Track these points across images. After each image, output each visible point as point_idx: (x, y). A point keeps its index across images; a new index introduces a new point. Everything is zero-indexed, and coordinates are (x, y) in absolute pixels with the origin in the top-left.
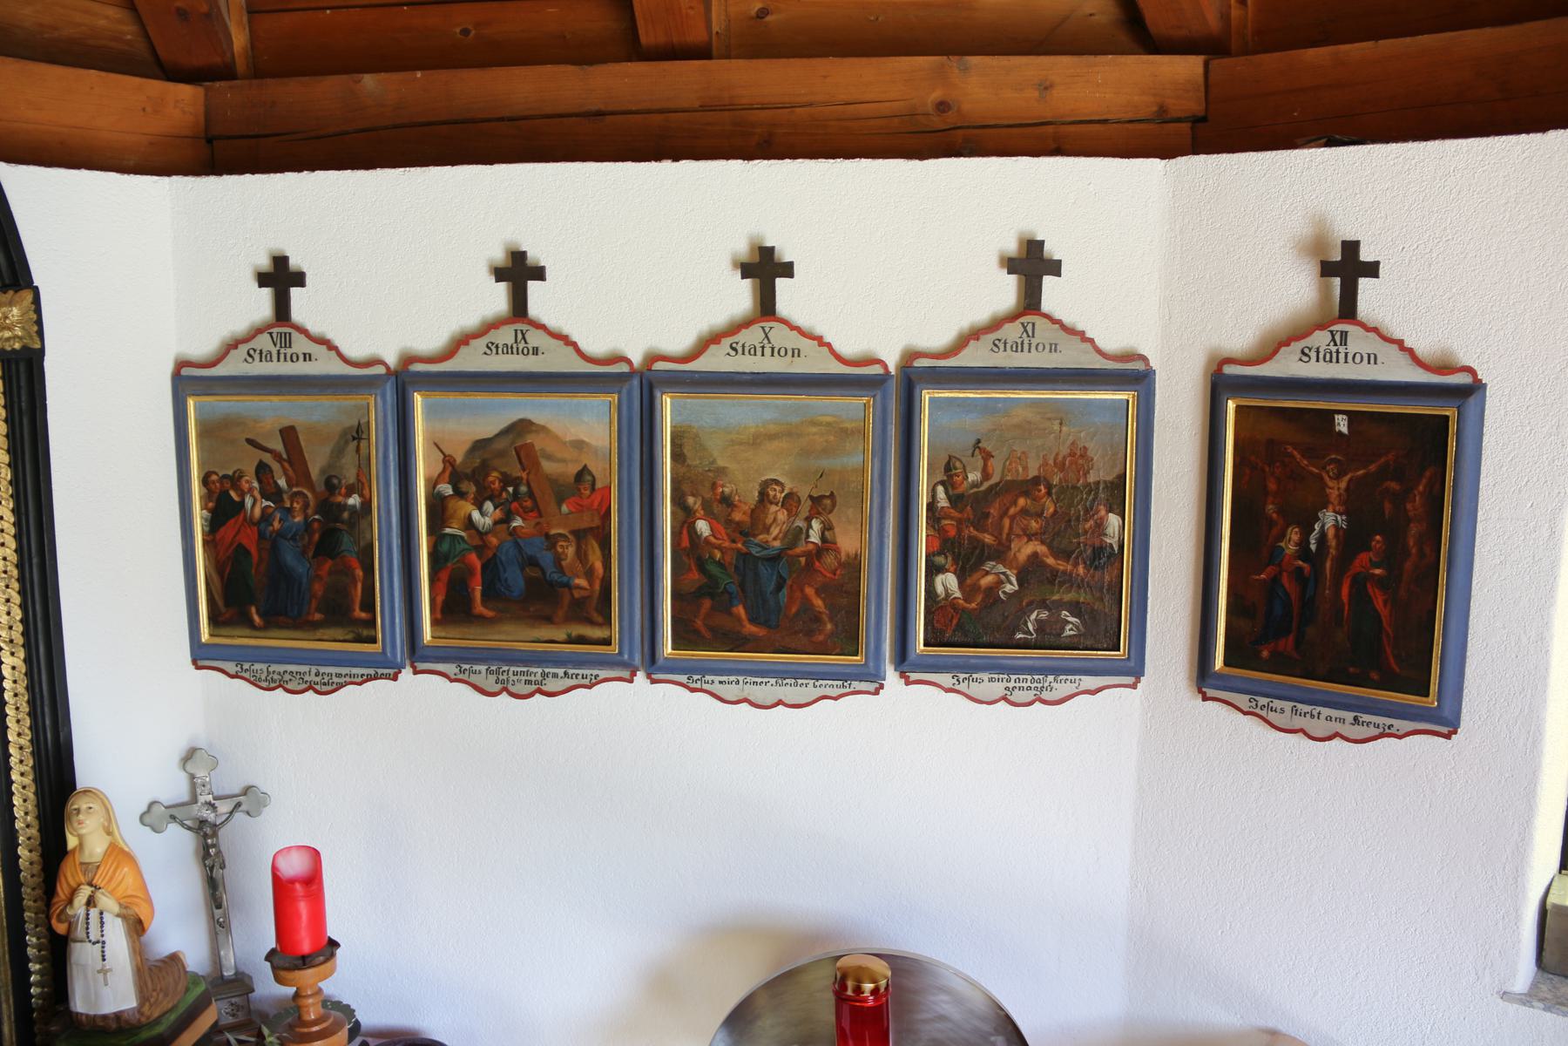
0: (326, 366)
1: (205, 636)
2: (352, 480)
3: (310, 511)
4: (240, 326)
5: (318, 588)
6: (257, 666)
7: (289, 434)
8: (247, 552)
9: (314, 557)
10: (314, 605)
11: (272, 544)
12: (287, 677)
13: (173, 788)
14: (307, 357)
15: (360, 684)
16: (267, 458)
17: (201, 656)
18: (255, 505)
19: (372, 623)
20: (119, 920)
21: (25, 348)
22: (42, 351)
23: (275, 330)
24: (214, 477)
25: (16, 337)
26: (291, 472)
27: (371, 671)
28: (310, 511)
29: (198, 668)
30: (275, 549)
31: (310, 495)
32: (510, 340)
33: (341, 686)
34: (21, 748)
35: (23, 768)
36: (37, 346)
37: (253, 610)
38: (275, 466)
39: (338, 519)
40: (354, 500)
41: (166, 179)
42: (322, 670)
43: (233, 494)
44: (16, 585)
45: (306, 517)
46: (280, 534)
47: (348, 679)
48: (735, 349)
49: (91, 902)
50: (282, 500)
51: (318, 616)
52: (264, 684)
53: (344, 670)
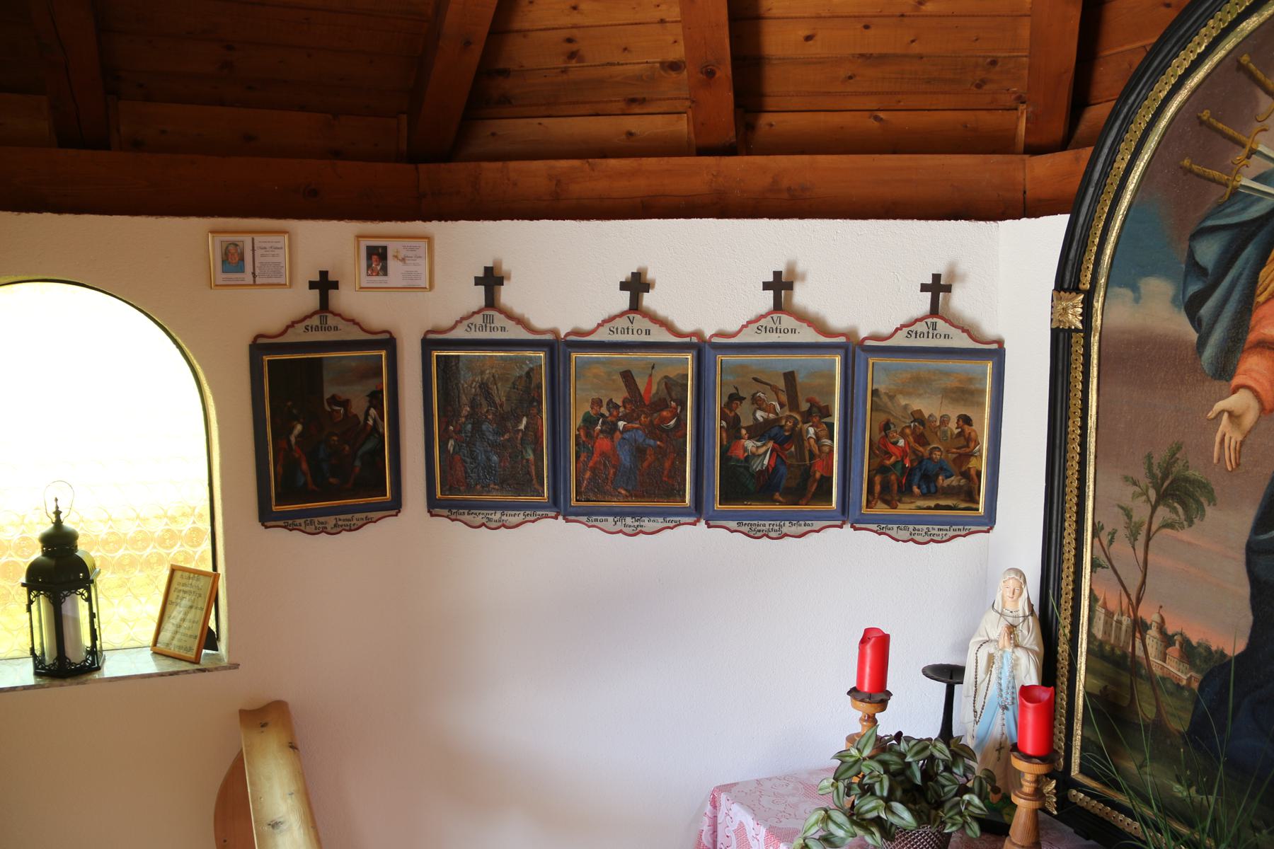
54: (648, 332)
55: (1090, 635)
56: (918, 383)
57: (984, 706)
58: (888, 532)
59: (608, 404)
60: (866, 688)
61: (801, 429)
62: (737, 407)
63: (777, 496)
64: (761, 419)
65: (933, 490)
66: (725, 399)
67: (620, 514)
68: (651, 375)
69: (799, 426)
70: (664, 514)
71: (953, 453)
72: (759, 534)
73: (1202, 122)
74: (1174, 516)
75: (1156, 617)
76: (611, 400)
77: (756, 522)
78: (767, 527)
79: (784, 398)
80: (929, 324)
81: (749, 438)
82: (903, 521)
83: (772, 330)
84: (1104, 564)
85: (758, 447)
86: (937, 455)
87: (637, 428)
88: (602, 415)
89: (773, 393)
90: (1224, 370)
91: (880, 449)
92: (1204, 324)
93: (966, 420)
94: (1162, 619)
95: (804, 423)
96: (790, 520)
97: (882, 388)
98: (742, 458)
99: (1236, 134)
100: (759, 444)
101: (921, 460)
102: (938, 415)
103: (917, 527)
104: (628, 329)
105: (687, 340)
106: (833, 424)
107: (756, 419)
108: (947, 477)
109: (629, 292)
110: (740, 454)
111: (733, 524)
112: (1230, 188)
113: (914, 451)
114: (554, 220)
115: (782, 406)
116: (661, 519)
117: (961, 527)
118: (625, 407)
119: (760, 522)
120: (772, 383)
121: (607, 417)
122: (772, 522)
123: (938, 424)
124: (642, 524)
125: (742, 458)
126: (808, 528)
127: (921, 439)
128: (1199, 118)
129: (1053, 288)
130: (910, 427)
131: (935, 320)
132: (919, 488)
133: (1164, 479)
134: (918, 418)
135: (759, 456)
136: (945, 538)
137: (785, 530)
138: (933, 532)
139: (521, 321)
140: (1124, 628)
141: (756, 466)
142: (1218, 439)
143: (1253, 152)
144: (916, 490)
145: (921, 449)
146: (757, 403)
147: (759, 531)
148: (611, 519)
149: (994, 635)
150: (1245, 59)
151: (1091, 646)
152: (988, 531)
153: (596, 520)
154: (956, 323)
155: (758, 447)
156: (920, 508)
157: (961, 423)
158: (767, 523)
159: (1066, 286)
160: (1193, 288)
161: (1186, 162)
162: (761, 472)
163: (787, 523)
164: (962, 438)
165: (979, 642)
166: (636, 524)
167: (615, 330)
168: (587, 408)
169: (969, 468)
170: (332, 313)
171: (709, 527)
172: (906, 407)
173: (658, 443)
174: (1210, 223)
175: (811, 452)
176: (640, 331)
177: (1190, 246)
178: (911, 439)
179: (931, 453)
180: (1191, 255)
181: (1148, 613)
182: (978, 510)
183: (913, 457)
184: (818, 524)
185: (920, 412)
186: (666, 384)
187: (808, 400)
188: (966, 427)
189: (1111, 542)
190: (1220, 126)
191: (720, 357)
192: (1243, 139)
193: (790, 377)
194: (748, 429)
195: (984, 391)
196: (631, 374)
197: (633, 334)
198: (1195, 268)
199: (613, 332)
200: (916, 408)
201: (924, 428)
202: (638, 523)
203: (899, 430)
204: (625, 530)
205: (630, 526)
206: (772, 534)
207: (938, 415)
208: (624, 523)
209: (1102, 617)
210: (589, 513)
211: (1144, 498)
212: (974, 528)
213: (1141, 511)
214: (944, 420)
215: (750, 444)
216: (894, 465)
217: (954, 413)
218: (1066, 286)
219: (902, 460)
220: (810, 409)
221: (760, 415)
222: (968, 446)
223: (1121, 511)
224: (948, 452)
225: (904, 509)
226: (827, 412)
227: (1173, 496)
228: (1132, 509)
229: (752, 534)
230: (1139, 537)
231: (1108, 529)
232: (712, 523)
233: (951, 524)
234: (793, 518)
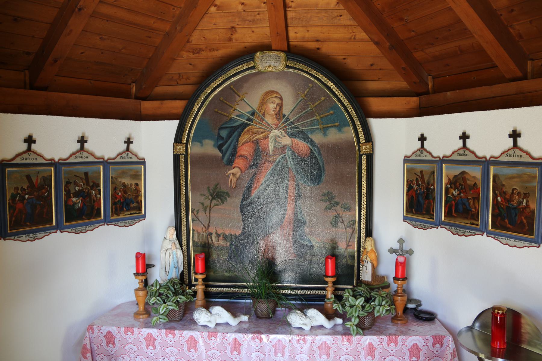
0: (429, 158)
1: (405, 214)
2: (432, 183)
3: (424, 189)
5: (425, 206)
6: (414, 222)
7: (422, 172)
8: (414, 197)
9: (425, 199)
10: (424, 210)
11: (418, 195)
12: (418, 225)
13: (396, 246)
14: (426, 156)
15: (431, 228)
16: (418, 177)
17: (405, 219)
18: (415, 187)
19: (433, 215)
20: (370, 263)
21: (369, 153)
22: (373, 154)
23: (421, 150)
24: (409, 181)
25: (368, 151)
26: (422, 181)
27: (433, 226)
28: (424, 189)
29: (404, 221)
30: (418, 197)
31: (425, 186)
32: (462, 153)
33: (427, 228)
34: (363, 229)
35: (363, 233)
36: (372, 153)
37: (414, 210)
38: (419, 179)
39: (429, 191)
40: (432, 187)
41: (405, 119)
42: (425, 224)
43: (412, 184)
44: (365, 198)
45: (424, 190)
46: (419, 194)
47: (429, 227)
48: (507, 155)
49: (366, 258)
50: (420, 186)
51: (424, 212)
52: (414, 226)
53: (428, 225)
54: (36, 159)
55: (194, 241)
56: (123, 173)
57: (169, 269)
58: (118, 224)
59: (21, 189)
60: (140, 272)
61: (90, 192)
62: (69, 186)
63: (84, 217)
64: (77, 190)
65: (129, 208)
66: (65, 183)
67: (27, 233)
68: (37, 176)
69: (90, 191)
70: (44, 230)
71: (134, 195)
72: (79, 232)
73: (220, 100)
74: (218, 202)
75: (215, 231)
76: (22, 187)
77: (77, 228)
78: (81, 229)
79: (84, 181)
80: (81, 153)
81: (74, 197)
82: (121, 220)
83: (80, 157)
84: (196, 220)
85: (77, 200)
86: (130, 197)
87: (33, 198)
88: (19, 194)
89: (81, 180)
90: (230, 162)
91: (114, 196)
92: (224, 152)
93: (137, 185)
94: (216, 231)
95: (91, 190)
96: (88, 225)
97: (114, 176)
98: (71, 205)
99: (230, 105)
100: (77, 199)
101: (125, 199)
102: (129, 184)
103: (126, 221)
104: (28, 158)
105: (50, 162)
106: (100, 190)
107: (76, 190)
108: (133, 204)
109: (27, 143)
110: (71, 203)
111: (69, 230)
112: (229, 117)
113: (124, 196)
114: (43, 115)
115: (84, 184)
116: (44, 233)
117: (137, 219)
118: (28, 189)
119: (79, 228)
120: (80, 176)
121: (21, 194)
122: (82, 227)
123: (129, 186)
124: (36, 235)
125: (71, 205)
126: (94, 227)
127: (125, 192)
128: (220, 99)
129: (173, 142)
130: (122, 188)
131: (128, 153)
132: (125, 208)
133: (213, 193)
134: (124, 185)
135: (77, 203)
136: (134, 224)
137: (87, 229)
138: (130, 222)
139: (93, 155)
140: (204, 236)
141: (77, 207)
142: (230, 180)
143: (235, 109)
144: (125, 209)
145: (125, 195)
146: (76, 184)
147: (79, 231)
148: (24, 236)
149: (169, 247)
150: (232, 87)
151: (194, 244)
152: (144, 220)
153: (18, 237)
154: (133, 153)
155: (77, 200)
156: (126, 215)
157: (136, 185)
158: (81, 227)
159: (178, 142)
160: (220, 142)
161: (216, 110)
162: (78, 209)
163: (87, 226)
164: (136, 191)
165: (166, 250)
166: (34, 236)
167: (23, 159)
168: (12, 191)
169: (139, 200)
170: (33, 152)
171: (61, 232)
172: (120, 182)
173: (41, 202)
174: (224, 126)
175: (94, 200)
176: (33, 159)
177: (218, 132)
178: (122, 192)
179: (128, 196)
180: (219, 134)
181: (212, 230)
182: (142, 213)
183: (123, 198)
184: (97, 225)
185: (124, 183)
186: (43, 179)
187: (92, 182)
188: (137, 187)
189: (198, 213)
190: (226, 102)
191: (63, 168)
192: (232, 106)
193: (86, 174)
194: (73, 194)
195: (141, 175)
196: (30, 176)
197: (30, 160)
198: (220, 137)
199: (22, 159)
200: (123, 182)
201: (126, 188)
202: (35, 236)
203: (119, 190)
204: (31, 239)
205: (32, 237)
206: (83, 231)
207: (129, 184)
208: (29, 236)
209: (197, 235)
210: (14, 235)
211: (208, 199)
212: (141, 219)
213: (207, 203)
214: (131, 185)
215: (74, 199)
216: (118, 201)
217: (133, 183)
218: (178, 142)
219: (120, 199)
220: (93, 184)
221: (77, 188)
222: (138, 193)
223: (200, 204)
224: (133, 195)
225: (122, 216)
226: (98, 185)
227: (218, 197)
228: (204, 203)
229: (76, 232)
230: (207, 210)
231: (196, 209)
232: (62, 231)
233: (135, 219)
234: (89, 224)
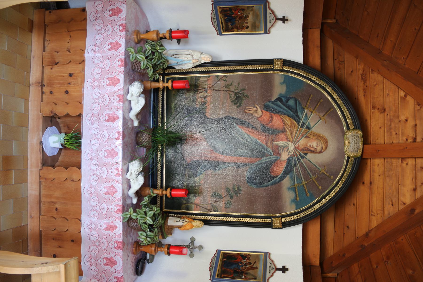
0: (268, 275)
1: (222, 251)
2: (247, 277)
3: (242, 270)
4: (276, 263)
5: (228, 270)
6: (215, 259)
7: (256, 268)
8: (236, 260)
9: (234, 270)
10: (225, 269)
11: (237, 263)
12: (213, 263)
13: (197, 243)
15: (210, 274)
16: (252, 264)
17: (218, 251)
18: (244, 262)
19: (221, 277)
20: (182, 225)
21: (273, 226)
22: (272, 228)
23: (275, 268)
24: (249, 256)
25: (275, 224)
26: (250, 268)
27: (212, 276)
28: (242, 270)
29: (217, 250)
30: (236, 264)
31: (245, 270)
33: (210, 271)
34: (211, 218)
35: (207, 218)
36: (273, 227)
37: (226, 259)
38: (251, 265)
39: (240, 274)
40: (243, 277)
41: (301, 254)
42: (213, 269)
43: (246, 259)
44: (236, 221)
45: (241, 269)
46: (239, 265)
47: (211, 272)
49: (186, 221)
50: (244, 266)
51: (223, 269)
52: (212, 259)
53: (213, 272)
55: (200, 77)
56: (256, 16)
58: (213, 12)
60: (173, 35)
65: (227, 22)
73: (320, 99)
75: (209, 95)
86: (237, 22)
90: (266, 108)
92: (275, 102)
93: (247, 27)
94: (209, 96)
97: (254, 8)
99: (316, 108)
101: (235, 18)
102: (248, 21)
103: (216, 19)
108: (231, 25)
113: (237, 17)
117: (218, 29)
123: (246, 21)
127: (241, 18)
131: (275, 20)
132: (227, 18)
134: (247, 17)
136: (214, 26)
143: (312, 112)
144: (226, 18)
145: (238, 18)
149: (195, 57)
150: (332, 110)
152: (218, 34)
154: (274, 24)
156: (221, 19)
160: (284, 99)
161: (312, 96)
172: (249, 14)
174: (298, 102)
178: (240, 16)
179: (237, 20)
180: (291, 98)
181: (210, 92)
182: (223, 32)
185: (249, 17)
188: (245, 28)
190: (319, 104)
192: (315, 110)
195: (256, 31)
198: (288, 99)
200: (249, 16)
203: (243, 13)
207: (248, 21)
209: (205, 80)
212: (218, 31)
213: (232, 88)
214: (247, 23)
216: (232, 12)
219: (234, 14)
222: (240, 28)
224: (238, 24)
225: (220, 16)
227: (237, 97)
230: (226, 88)
231: (227, 79)
233: (218, 26)
